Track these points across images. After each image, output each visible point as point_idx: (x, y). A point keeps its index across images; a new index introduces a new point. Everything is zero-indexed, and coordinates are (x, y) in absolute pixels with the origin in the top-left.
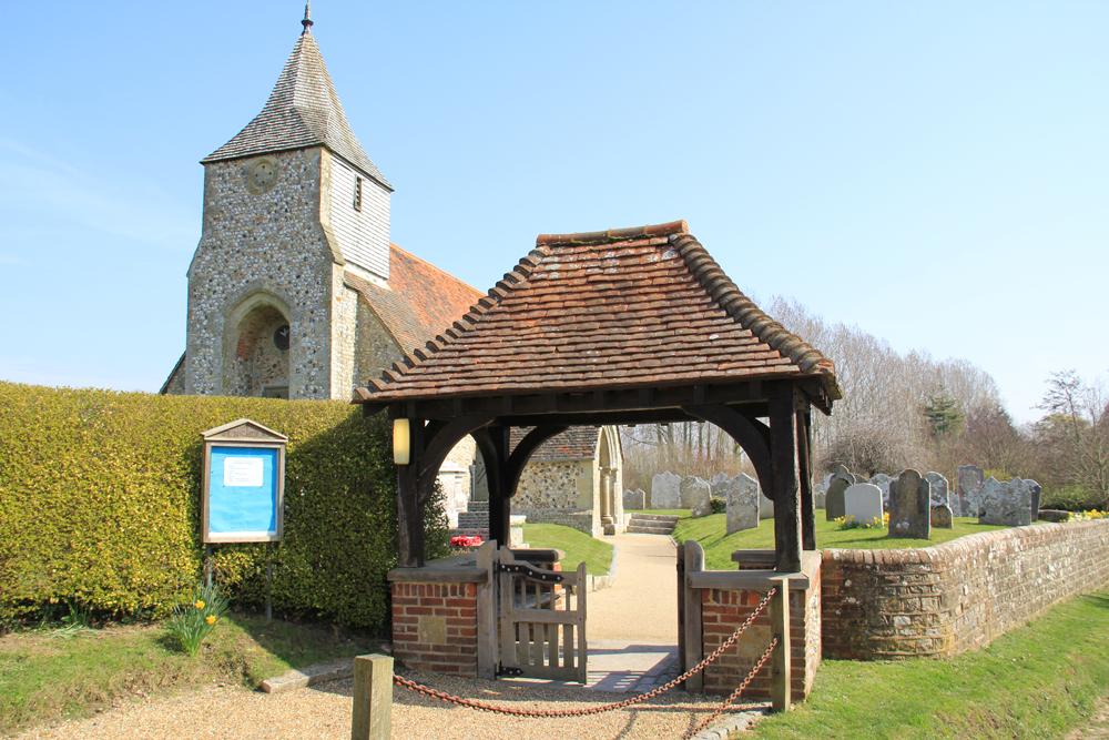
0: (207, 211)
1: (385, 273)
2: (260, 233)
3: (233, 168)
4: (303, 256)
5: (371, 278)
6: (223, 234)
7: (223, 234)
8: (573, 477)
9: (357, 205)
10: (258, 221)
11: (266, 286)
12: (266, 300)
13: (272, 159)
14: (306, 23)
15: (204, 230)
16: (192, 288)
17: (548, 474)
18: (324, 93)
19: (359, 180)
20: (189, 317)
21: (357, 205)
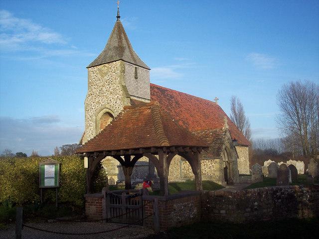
0: (89, 83)
1: (149, 97)
2: (104, 89)
3: (96, 68)
4: (117, 96)
5: (143, 100)
6: (94, 90)
7: (94, 90)
8: (213, 164)
9: (136, 78)
10: (103, 86)
11: (107, 106)
12: (108, 110)
13: (107, 65)
14: (118, 17)
15: (88, 89)
16: (86, 108)
17: (205, 163)
18: (124, 41)
19: (136, 68)
20: (85, 117)
21: (136, 78)
